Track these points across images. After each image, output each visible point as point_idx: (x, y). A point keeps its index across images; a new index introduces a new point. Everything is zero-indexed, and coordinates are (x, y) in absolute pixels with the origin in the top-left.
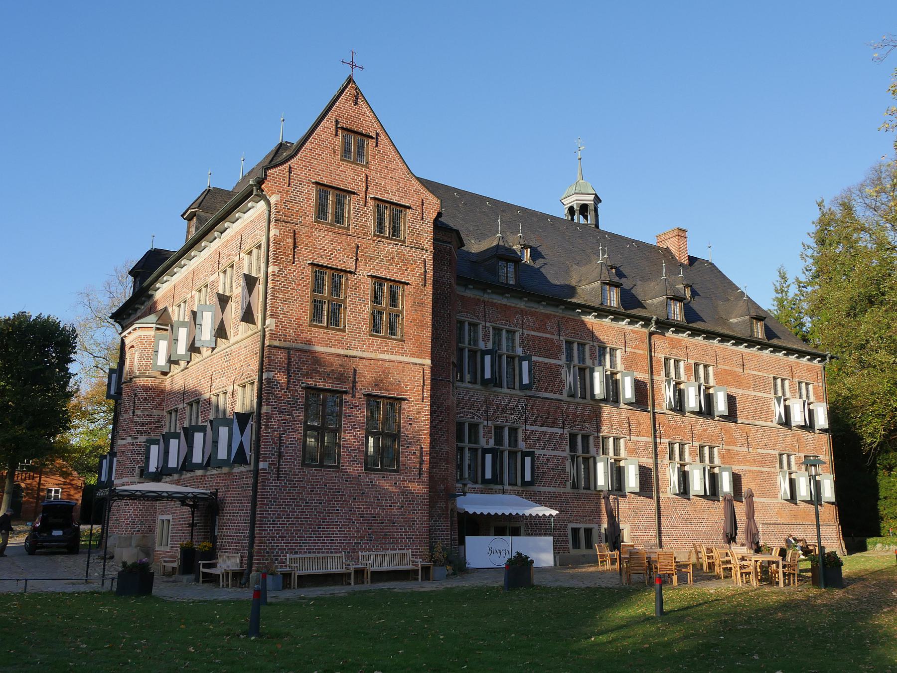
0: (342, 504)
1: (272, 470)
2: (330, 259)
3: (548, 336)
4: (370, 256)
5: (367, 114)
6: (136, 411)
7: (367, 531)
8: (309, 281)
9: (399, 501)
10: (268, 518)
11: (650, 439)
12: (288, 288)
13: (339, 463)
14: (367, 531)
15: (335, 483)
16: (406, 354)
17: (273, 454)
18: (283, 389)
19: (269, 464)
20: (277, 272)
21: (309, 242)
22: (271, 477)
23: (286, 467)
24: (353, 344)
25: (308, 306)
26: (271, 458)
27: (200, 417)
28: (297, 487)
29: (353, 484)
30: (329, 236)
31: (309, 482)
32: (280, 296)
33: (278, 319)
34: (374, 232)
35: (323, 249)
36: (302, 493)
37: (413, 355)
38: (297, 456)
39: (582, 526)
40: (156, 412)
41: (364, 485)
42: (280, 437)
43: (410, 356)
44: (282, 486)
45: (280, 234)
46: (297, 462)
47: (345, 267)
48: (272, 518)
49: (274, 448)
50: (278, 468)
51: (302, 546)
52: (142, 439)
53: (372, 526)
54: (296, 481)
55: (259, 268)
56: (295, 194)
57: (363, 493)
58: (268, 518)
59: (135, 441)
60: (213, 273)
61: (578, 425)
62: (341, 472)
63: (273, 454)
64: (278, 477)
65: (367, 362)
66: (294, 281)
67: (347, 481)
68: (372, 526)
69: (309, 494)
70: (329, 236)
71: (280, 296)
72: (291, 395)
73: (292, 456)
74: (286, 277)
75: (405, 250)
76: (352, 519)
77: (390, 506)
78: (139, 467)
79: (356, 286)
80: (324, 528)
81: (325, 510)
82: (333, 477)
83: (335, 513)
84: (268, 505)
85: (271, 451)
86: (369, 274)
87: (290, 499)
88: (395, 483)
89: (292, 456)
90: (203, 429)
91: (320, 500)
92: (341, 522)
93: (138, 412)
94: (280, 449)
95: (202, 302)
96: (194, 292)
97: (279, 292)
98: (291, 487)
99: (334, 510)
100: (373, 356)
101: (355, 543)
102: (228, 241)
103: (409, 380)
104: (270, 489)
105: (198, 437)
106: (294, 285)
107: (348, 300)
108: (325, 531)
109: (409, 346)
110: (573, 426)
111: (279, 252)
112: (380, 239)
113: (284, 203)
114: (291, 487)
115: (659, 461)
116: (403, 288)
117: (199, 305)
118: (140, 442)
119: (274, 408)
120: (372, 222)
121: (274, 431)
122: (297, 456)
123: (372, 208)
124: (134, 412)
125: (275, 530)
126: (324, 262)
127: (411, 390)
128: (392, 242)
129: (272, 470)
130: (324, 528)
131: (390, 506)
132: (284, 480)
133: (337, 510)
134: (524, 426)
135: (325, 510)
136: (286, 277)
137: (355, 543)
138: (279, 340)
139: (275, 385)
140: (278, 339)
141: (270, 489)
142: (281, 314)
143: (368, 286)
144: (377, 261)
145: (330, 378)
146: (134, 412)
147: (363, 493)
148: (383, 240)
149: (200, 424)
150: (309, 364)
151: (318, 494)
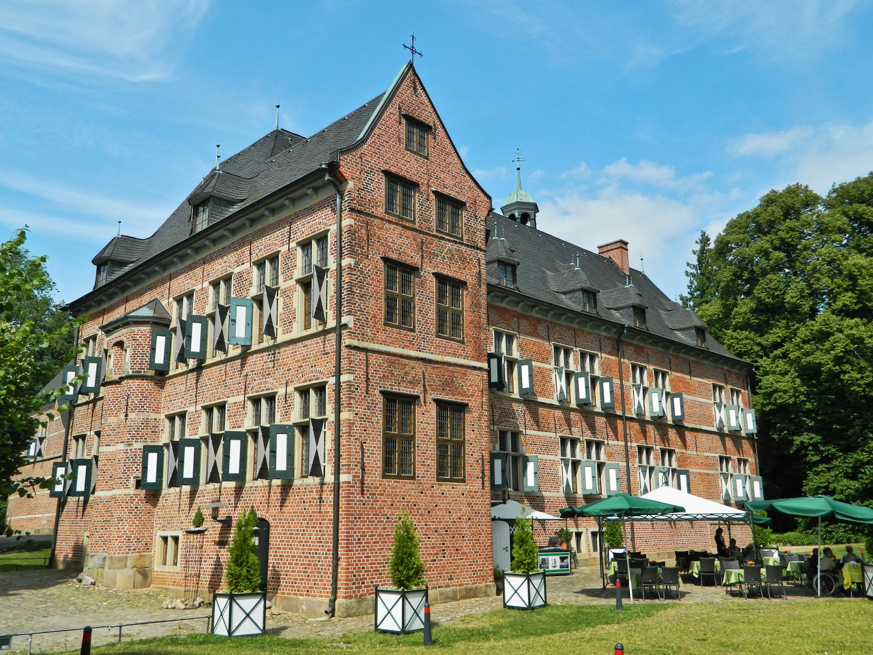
1: (356, 483)
10: (353, 536)
13: (414, 474)
16: (466, 357)
18: (363, 393)
28: (378, 501)
37: (473, 358)
42: (362, 446)
46: (379, 471)
48: (357, 536)
58: (353, 536)
63: (356, 466)
66: (369, 276)
67: (422, 493)
69: (389, 508)
72: (371, 400)
79: (422, 284)
86: (434, 271)
87: (374, 515)
89: (373, 467)
104: (355, 504)
114: (373, 501)
121: (356, 439)
122: (378, 467)
125: (361, 550)
126: (394, 256)
141: (355, 504)
145: (404, 381)
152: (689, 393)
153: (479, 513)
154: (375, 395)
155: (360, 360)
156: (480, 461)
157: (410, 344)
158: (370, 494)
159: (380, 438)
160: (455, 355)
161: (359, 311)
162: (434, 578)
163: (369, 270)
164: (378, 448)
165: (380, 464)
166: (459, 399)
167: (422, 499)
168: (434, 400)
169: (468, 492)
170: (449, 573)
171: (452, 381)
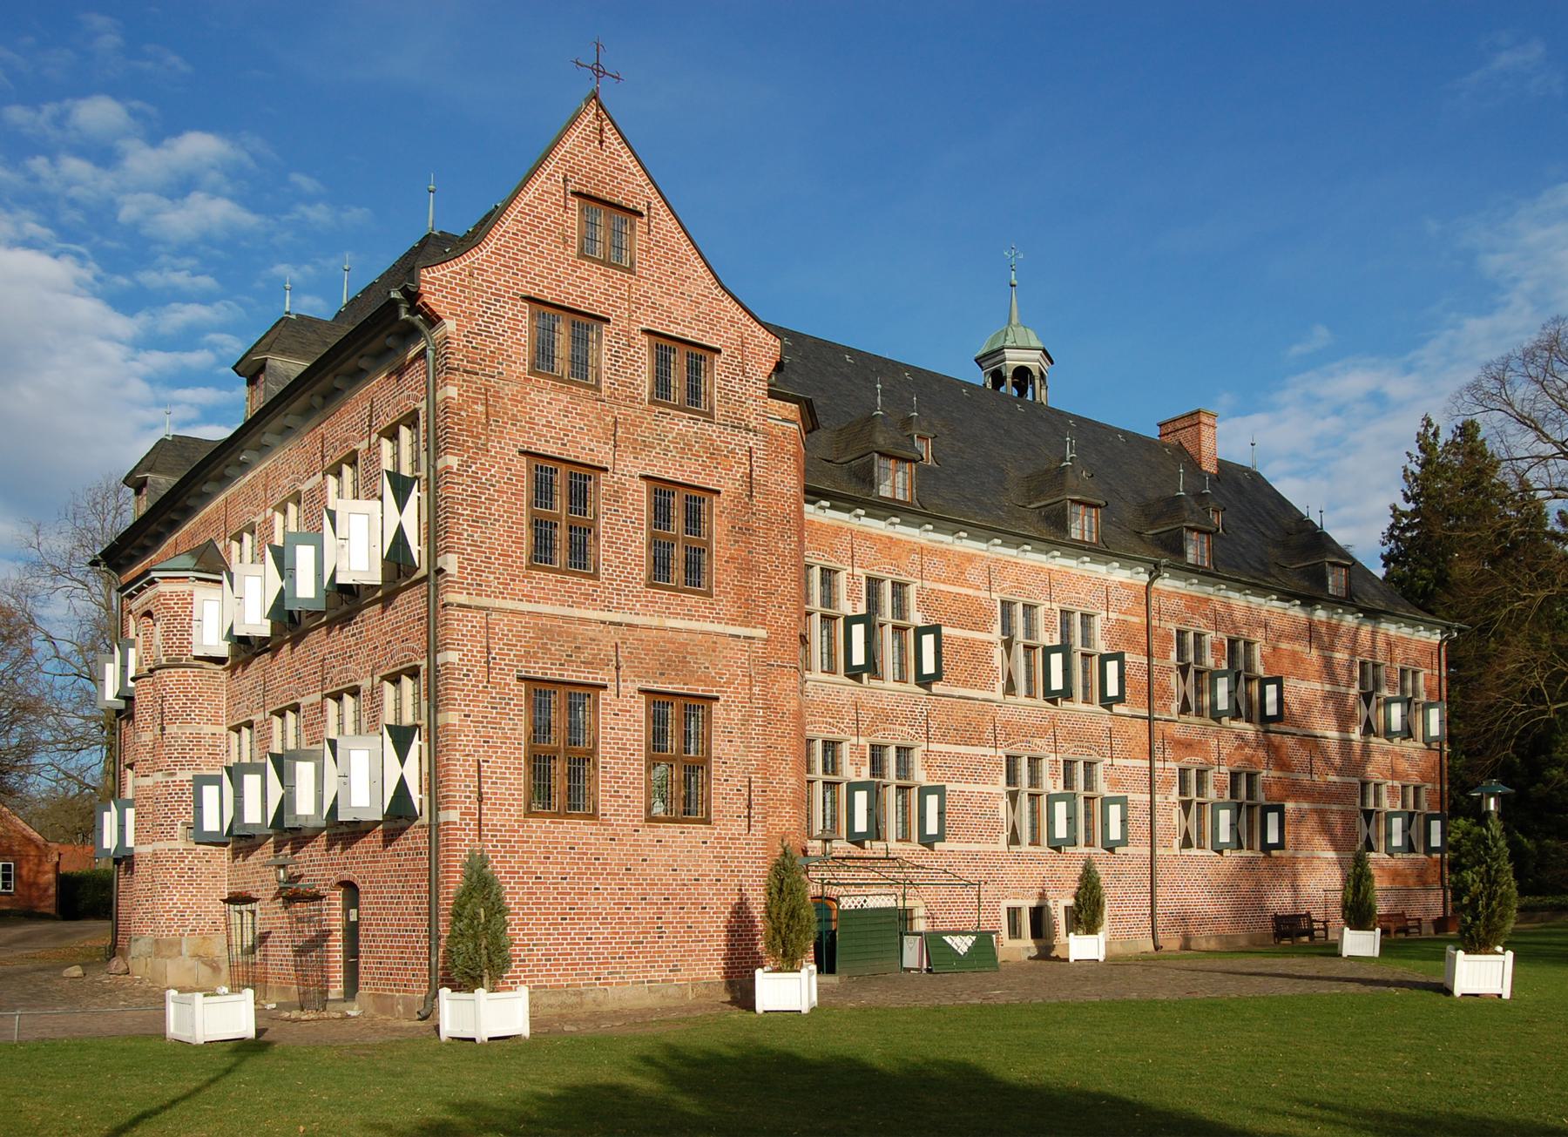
4: (644, 441)
8: (524, 486)
16: (719, 620)
19: (462, 814)
20: (456, 467)
23: (492, 818)
25: (526, 534)
34: (651, 394)
35: (548, 424)
37: (733, 621)
62: (601, 824)
75: (712, 430)
79: (616, 496)
107: (602, 522)
109: (725, 605)
112: (661, 409)
116: (711, 500)
123: (645, 350)
127: (729, 683)
128: (687, 415)
136: (475, 479)
143: (640, 497)
148: (668, 411)
156: (745, 791)
159: (521, 754)
160: (691, 617)
166: (700, 690)
168: (642, 691)
171: (684, 661)
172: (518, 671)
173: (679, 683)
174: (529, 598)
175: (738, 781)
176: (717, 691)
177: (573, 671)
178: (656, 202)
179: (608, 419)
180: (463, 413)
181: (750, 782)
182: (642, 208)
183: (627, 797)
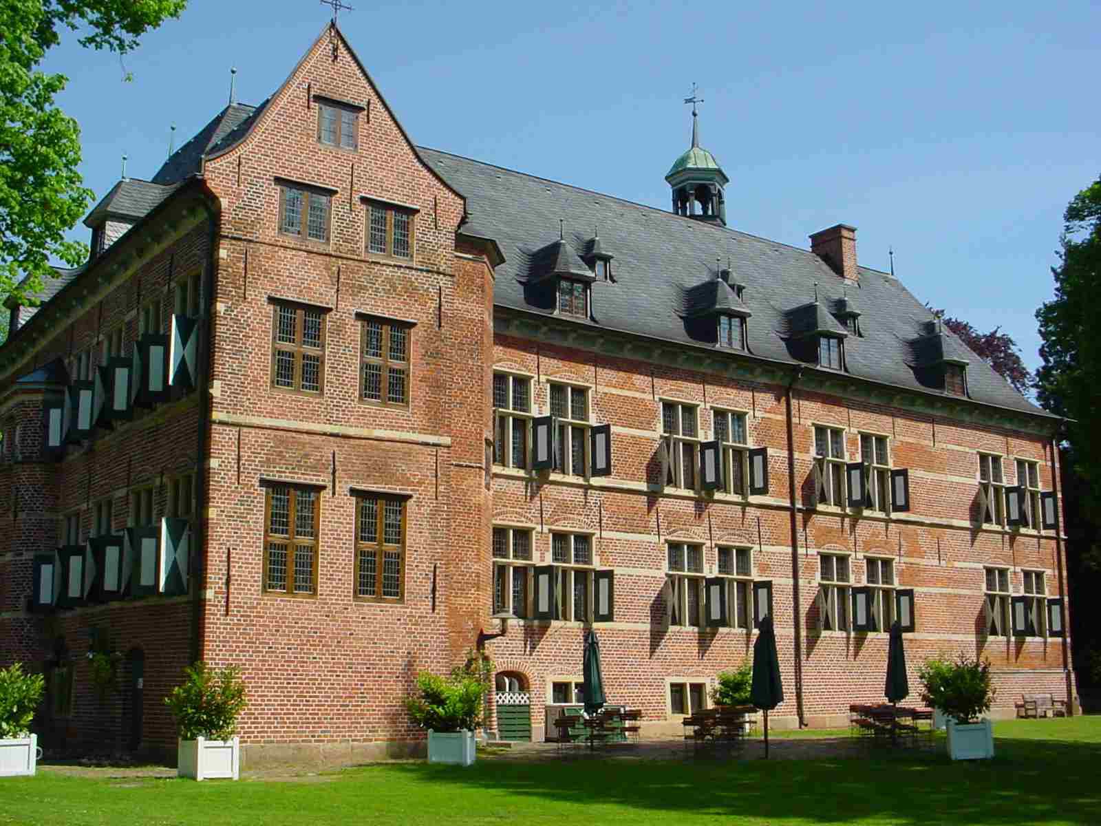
0: (321, 650)
2: (301, 291)
3: (637, 395)
5: (356, 75)
6: (20, 514)
7: (358, 689)
9: (404, 645)
11: (790, 550)
12: (238, 335)
14: (358, 689)
15: (310, 619)
16: (413, 429)
17: (220, 579)
19: (216, 592)
21: (269, 266)
22: (219, 610)
24: (335, 416)
26: (218, 583)
27: (113, 523)
29: (337, 621)
30: (299, 256)
31: (273, 618)
32: (228, 347)
33: (225, 380)
36: (262, 634)
37: (423, 430)
38: (255, 581)
39: (688, 680)
40: (47, 516)
41: (353, 621)
43: (420, 433)
44: (234, 624)
45: (228, 256)
47: (321, 302)
49: (221, 570)
50: (228, 598)
51: (264, 709)
52: (28, 556)
53: (366, 681)
54: (254, 617)
55: (196, 306)
56: (249, 196)
57: (351, 634)
59: (18, 558)
60: (129, 309)
61: (682, 530)
63: (220, 579)
64: (227, 611)
65: (352, 442)
66: (249, 325)
68: (366, 681)
70: (299, 256)
71: (228, 347)
73: (248, 581)
74: (236, 320)
76: (336, 671)
77: (391, 652)
78: (25, 597)
79: (339, 330)
80: (296, 683)
81: (296, 658)
82: (307, 611)
83: (311, 663)
84: (215, 650)
85: (218, 574)
88: (399, 620)
89: (248, 581)
90: (118, 542)
91: (289, 644)
92: (320, 675)
93: (22, 516)
94: (228, 570)
95: (113, 354)
96: (101, 337)
97: (225, 341)
98: (247, 625)
99: (308, 658)
100: (364, 432)
101: (341, 706)
102: (150, 264)
103: (418, 468)
105: (112, 553)
106: (247, 330)
108: (297, 688)
109: (418, 420)
110: (675, 531)
111: (226, 283)
113: (234, 210)
115: (801, 582)
117: (111, 359)
118: (26, 560)
119: (221, 511)
120: (363, 234)
122: (255, 581)
124: (16, 516)
127: (420, 483)
129: (219, 602)
130: (296, 683)
131: (391, 652)
132: (236, 616)
133: (314, 658)
134: (598, 532)
135: (296, 658)
137: (341, 706)
138: (227, 412)
139: (222, 478)
140: (225, 410)
142: (229, 373)
143: (355, 331)
144: (370, 292)
146: (16, 516)
147: (351, 634)
149: (114, 533)
150: (271, 447)
151: (286, 635)
152: (929, 468)
153: (426, 646)
154: (253, 485)
155: (230, 439)
156: (431, 576)
157: (314, 415)
158: (242, 616)
161: (229, 373)
162: (344, 727)
163: (249, 318)
164: (256, 555)
165: (259, 577)
166: (397, 489)
167: (328, 625)
168: (353, 492)
169: (408, 616)
170: (370, 723)
172: (261, 474)
173: (381, 483)
174: (271, 414)
175: (427, 567)
176: (412, 490)
177: (302, 474)
178: (374, 99)
179: (334, 268)
180: (230, 270)
181: (435, 567)
182: (363, 104)
183: (340, 580)
